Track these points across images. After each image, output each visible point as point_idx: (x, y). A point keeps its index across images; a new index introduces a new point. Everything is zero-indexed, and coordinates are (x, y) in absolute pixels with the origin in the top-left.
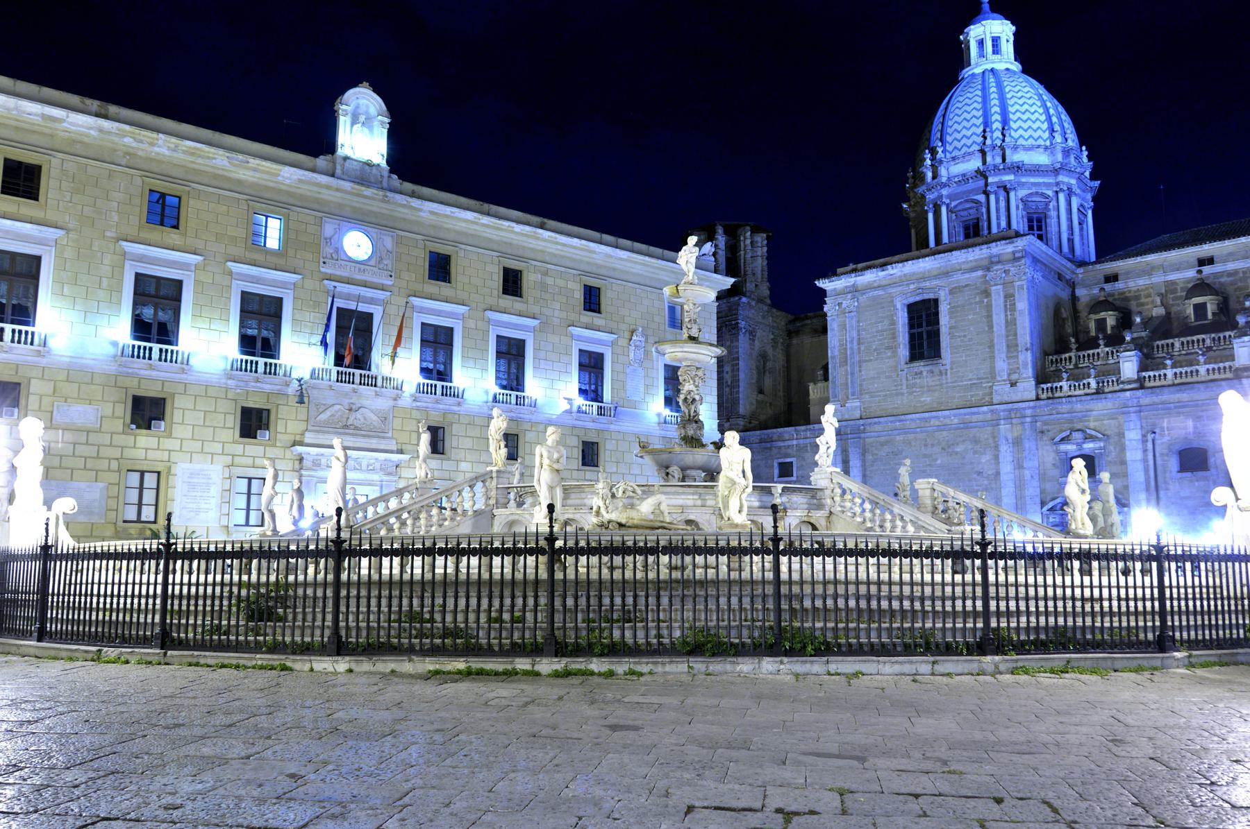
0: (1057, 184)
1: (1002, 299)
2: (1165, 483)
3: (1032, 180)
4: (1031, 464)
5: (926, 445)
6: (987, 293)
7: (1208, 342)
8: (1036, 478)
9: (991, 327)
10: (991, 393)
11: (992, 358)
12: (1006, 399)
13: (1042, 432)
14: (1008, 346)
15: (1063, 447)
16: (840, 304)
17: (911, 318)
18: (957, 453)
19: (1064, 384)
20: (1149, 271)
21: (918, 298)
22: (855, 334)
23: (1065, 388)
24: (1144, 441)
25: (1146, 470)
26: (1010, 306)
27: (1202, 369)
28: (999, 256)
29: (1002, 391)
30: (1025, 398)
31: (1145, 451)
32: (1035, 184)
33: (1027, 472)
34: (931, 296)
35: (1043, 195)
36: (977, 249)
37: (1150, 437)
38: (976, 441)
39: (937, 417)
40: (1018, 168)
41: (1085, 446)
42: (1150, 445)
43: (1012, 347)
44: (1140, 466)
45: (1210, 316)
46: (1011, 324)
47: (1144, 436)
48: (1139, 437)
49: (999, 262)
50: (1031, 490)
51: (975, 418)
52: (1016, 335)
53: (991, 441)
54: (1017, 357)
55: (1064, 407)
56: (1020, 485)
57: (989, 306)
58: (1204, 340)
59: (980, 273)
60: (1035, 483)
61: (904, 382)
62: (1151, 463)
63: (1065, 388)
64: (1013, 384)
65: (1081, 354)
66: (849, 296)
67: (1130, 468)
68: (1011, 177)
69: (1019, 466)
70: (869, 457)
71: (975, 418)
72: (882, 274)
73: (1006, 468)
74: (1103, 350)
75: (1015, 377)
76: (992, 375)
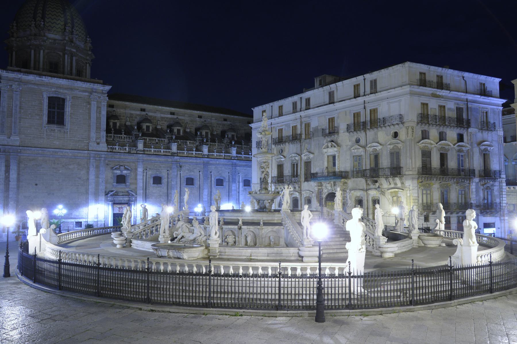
1: (96, 108)
5: (54, 163)
6: (89, 103)
7: (157, 141)
9: (90, 118)
11: (89, 131)
12: (96, 150)
13: (108, 164)
15: (115, 171)
16: (11, 86)
17: (49, 103)
18: (70, 169)
19: (117, 147)
20: (125, 108)
21: (55, 96)
22: (18, 103)
23: (117, 149)
24: (144, 173)
25: (143, 183)
26: (99, 112)
27: (153, 150)
28: (96, 89)
29: (93, 146)
30: (103, 150)
34: (62, 97)
36: (89, 84)
37: (145, 171)
39: (62, 152)
42: (145, 174)
43: (98, 128)
44: (141, 181)
45: (151, 130)
46: (98, 119)
49: (96, 92)
51: (79, 155)
52: (100, 124)
54: (100, 133)
55: (117, 156)
56: (97, 184)
57: (90, 109)
59: (87, 94)
61: (45, 132)
63: (117, 149)
64: (98, 144)
65: (115, 135)
66: (17, 83)
68: (75, 51)
69: (97, 177)
70: (22, 166)
71: (79, 155)
72: (38, 78)
73: (92, 177)
74: (123, 136)
75: (98, 141)
76: (89, 138)
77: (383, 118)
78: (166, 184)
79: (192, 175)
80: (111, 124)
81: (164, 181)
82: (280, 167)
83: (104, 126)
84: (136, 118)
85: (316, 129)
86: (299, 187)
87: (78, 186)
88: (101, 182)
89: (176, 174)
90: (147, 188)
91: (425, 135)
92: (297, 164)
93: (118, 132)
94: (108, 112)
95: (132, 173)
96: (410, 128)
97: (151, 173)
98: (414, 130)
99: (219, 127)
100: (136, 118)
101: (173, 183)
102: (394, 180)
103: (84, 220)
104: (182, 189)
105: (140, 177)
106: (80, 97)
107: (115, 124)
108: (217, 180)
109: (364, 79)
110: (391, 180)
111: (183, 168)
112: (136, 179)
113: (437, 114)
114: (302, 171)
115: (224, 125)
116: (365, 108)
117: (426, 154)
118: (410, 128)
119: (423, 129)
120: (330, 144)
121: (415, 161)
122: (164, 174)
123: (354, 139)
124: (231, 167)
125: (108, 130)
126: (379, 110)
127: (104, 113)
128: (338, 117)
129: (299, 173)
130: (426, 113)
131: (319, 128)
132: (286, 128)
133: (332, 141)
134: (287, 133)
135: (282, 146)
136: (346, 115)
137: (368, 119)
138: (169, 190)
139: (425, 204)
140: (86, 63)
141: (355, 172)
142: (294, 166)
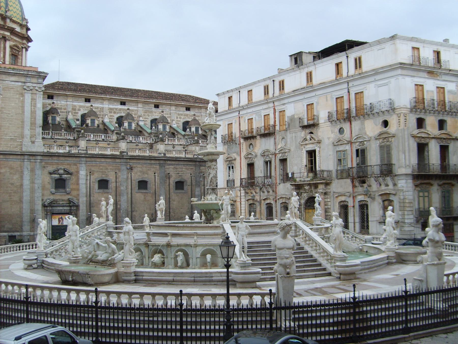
0: (23, 44)
1: (30, 100)
2: (93, 194)
3: (15, 38)
4: (38, 182)
6: (22, 95)
7: (103, 137)
8: (40, 188)
9: (23, 112)
10: (22, 145)
11: (23, 127)
13: (44, 167)
14: (31, 123)
15: (53, 175)
23: (55, 148)
26: (33, 105)
31: (87, 180)
32: (16, 41)
33: (36, 185)
35: (18, 47)
38: (11, 168)
40: (12, 31)
41: (63, 176)
43: (33, 124)
44: (84, 186)
46: (33, 113)
47: (87, 174)
48: (85, 174)
50: (38, 194)
52: (35, 119)
53: (19, 169)
54: (35, 129)
57: (23, 102)
58: (101, 136)
59: (20, 84)
60: (40, 191)
62: (88, 185)
64: (33, 142)
67: (80, 187)
73: (26, 182)
75: (33, 139)
76: (22, 136)
77: (371, 104)
78: (114, 189)
79: (145, 177)
80: (50, 119)
81: (112, 185)
82: (251, 166)
83: (40, 121)
84: (79, 110)
85: (292, 119)
86: (273, 191)
87: (11, 193)
88: (36, 188)
89: (125, 177)
90: (92, 195)
91: (420, 123)
92: (270, 162)
93: (57, 127)
94: (44, 105)
95: (74, 177)
96: (402, 115)
97: (97, 176)
98: (407, 118)
99: (180, 118)
100: (79, 110)
101: (122, 188)
102: (384, 180)
103: (19, 234)
104: (133, 195)
105: (82, 181)
106: (13, 88)
107: (54, 119)
108: (176, 183)
109: (347, 57)
110: (381, 179)
111: (135, 170)
112: (78, 184)
113: (435, 98)
114: (276, 171)
115: (187, 115)
116: (349, 92)
117: (422, 148)
118: (402, 115)
119: (418, 117)
120: (308, 137)
121: (409, 156)
122: (111, 177)
123: (337, 130)
124: (194, 168)
125: (45, 125)
126: (366, 94)
127: (39, 105)
128: (318, 103)
129: (273, 174)
130: (421, 96)
131: (296, 117)
132: (257, 118)
133: (311, 133)
134: (258, 124)
135: (252, 141)
136: (327, 100)
137: (353, 105)
138: (118, 197)
139: (422, 210)
140: (22, 47)
141: (339, 172)
142: (268, 163)
